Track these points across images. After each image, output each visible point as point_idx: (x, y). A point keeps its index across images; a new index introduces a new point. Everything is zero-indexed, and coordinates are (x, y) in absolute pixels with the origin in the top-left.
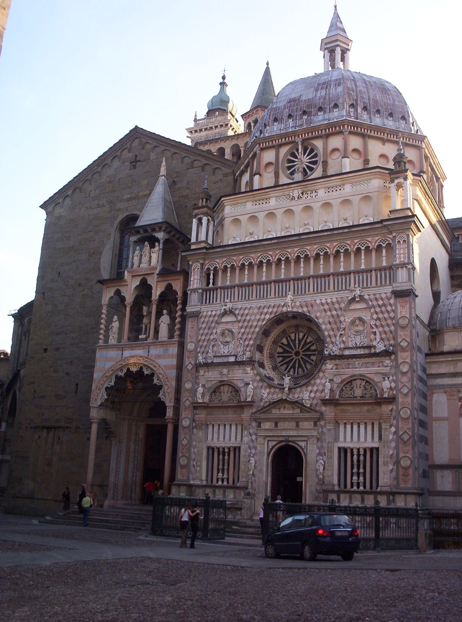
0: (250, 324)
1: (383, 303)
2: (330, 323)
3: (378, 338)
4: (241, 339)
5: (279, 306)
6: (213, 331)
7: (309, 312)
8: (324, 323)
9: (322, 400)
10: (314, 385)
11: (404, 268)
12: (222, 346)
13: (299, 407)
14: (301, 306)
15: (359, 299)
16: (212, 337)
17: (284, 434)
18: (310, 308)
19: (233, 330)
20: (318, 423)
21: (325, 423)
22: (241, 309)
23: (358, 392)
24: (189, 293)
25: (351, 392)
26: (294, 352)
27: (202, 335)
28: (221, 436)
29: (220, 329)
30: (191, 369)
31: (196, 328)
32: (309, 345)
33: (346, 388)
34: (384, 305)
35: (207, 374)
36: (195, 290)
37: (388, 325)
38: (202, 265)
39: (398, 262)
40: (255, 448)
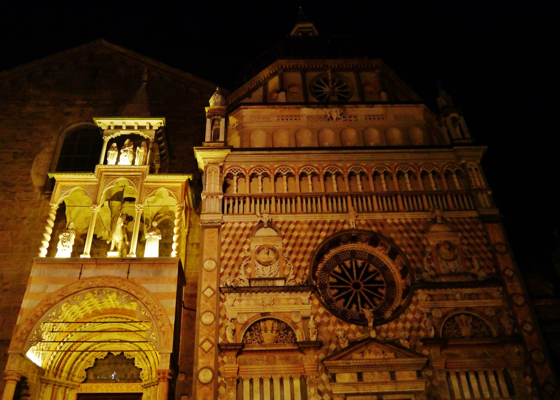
0: (300, 241)
2: (410, 246)
3: (477, 267)
4: (288, 259)
7: (379, 230)
8: (403, 246)
9: (423, 340)
11: (485, 195)
12: (260, 266)
13: (391, 350)
16: (242, 255)
18: (380, 228)
19: (276, 247)
20: (423, 373)
22: (283, 223)
23: (465, 331)
24: (203, 197)
25: (456, 331)
26: (351, 284)
27: (226, 251)
30: (212, 296)
31: (216, 243)
32: (372, 276)
33: (448, 325)
35: (237, 303)
36: (212, 196)
38: (222, 168)
39: (475, 187)
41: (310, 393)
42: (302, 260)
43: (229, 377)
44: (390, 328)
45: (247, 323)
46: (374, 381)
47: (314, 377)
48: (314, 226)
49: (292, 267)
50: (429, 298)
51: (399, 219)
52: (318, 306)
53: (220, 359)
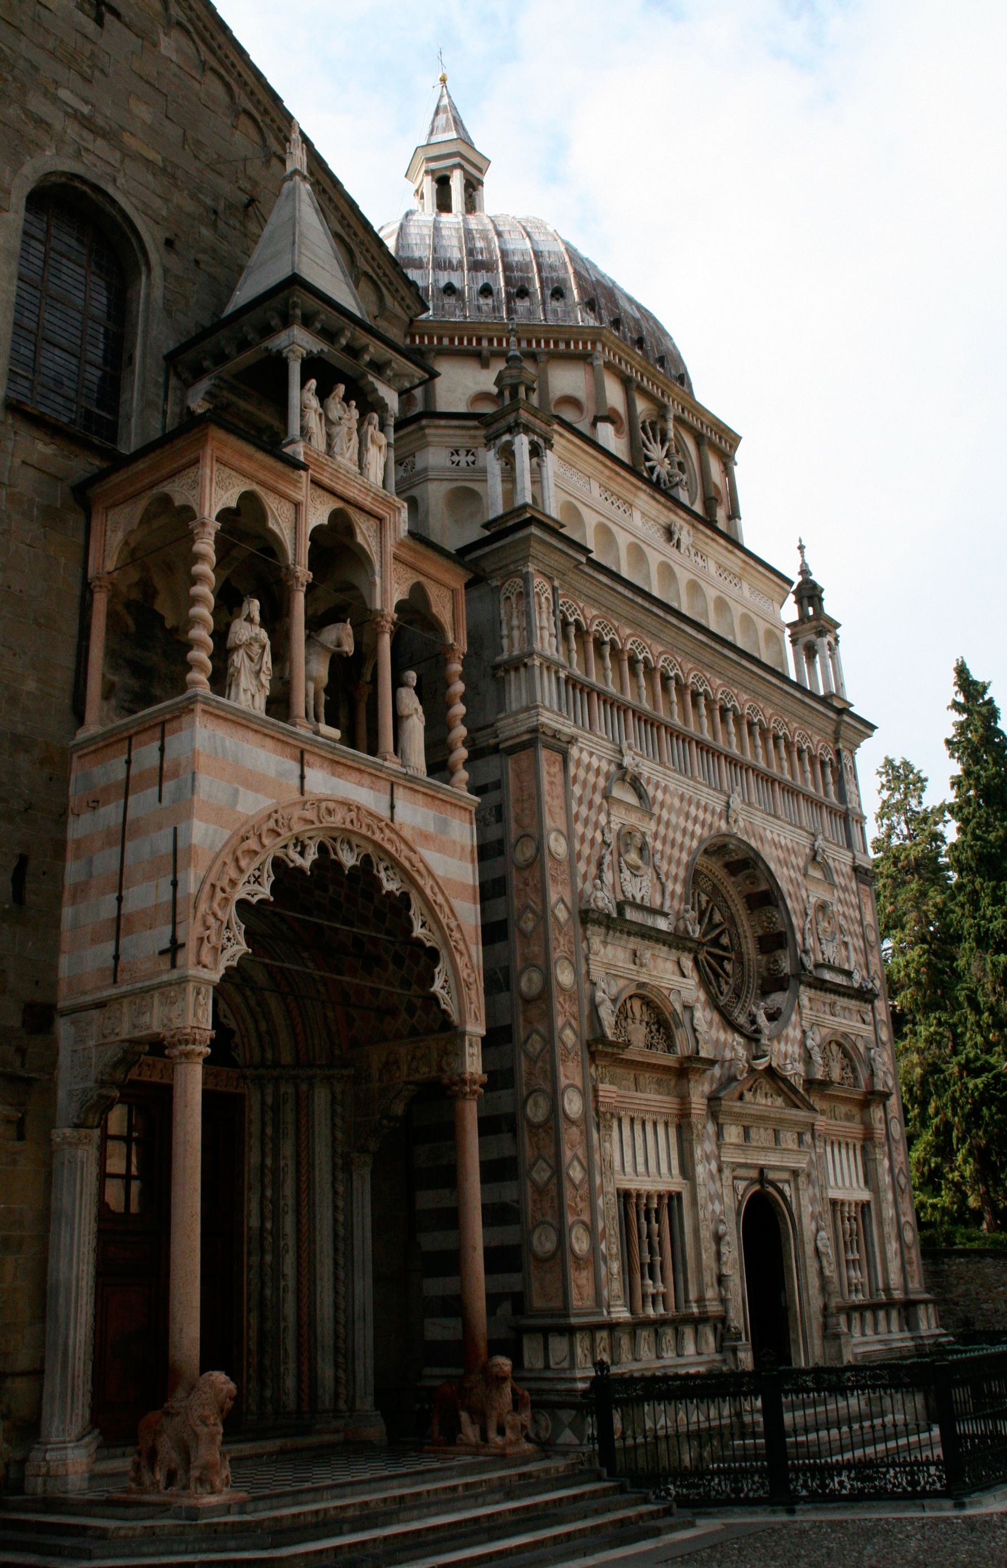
12: (627, 874)
13: (780, 1092)
14: (747, 833)
18: (759, 843)
28: (640, 1160)
35: (602, 950)
40: (720, 1198)
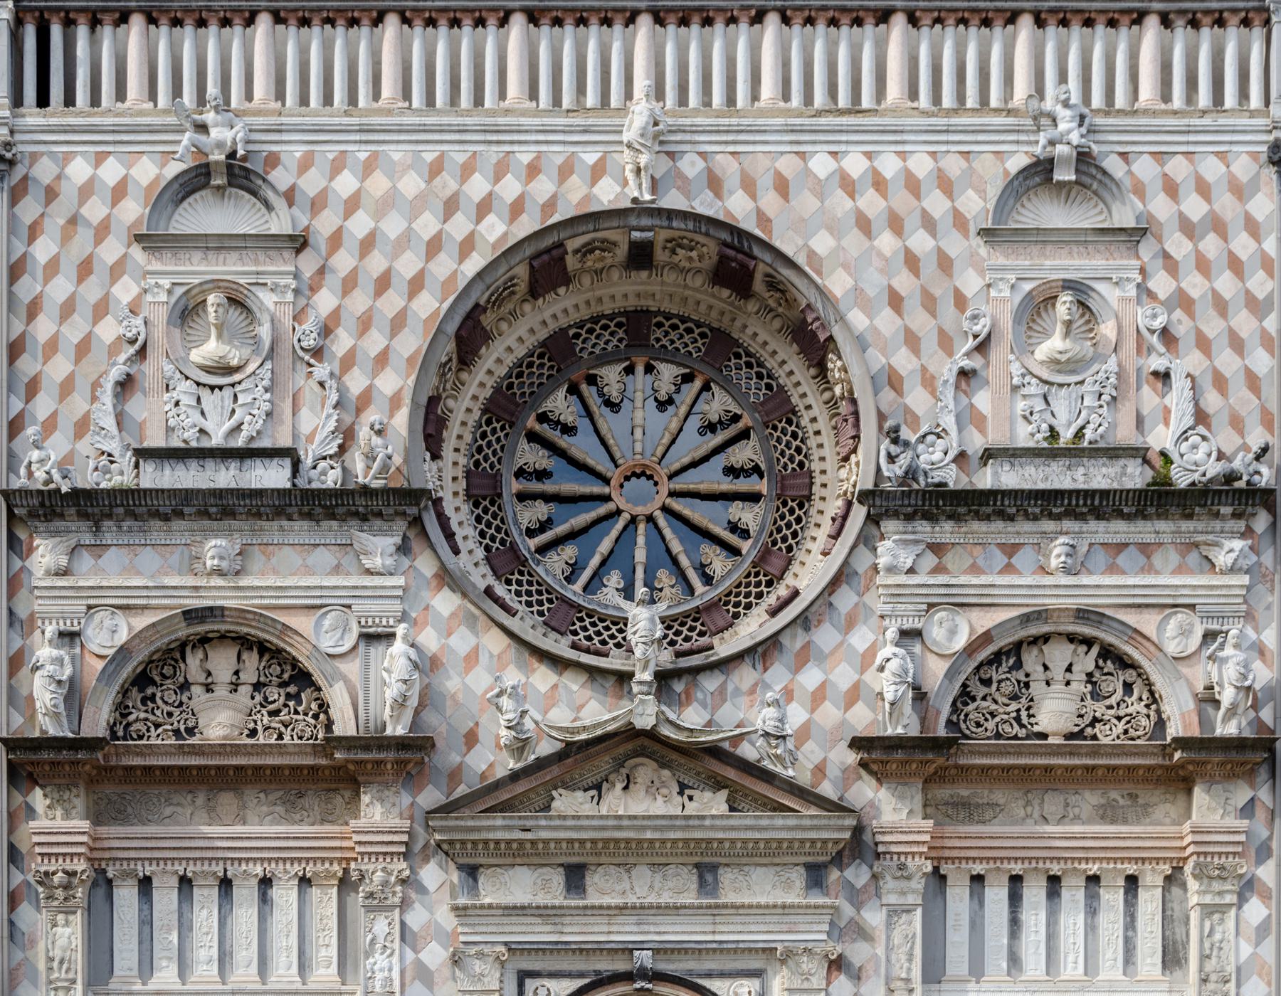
0: (376, 263)
1: (1212, 213)
2: (896, 301)
4: (318, 353)
5: (565, 171)
6: (117, 290)
7: (763, 219)
10: (802, 659)
15: (1073, 178)
17: (625, 932)
18: (770, 201)
20: (834, 874)
21: (875, 877)
29: (166, 282)
34: (1218, 226)
35: (86, 561)
37: (1237, 344)
41: (370, 937)
42: (382, 360)
43: (52, 869)
44: (730, 687)
45: (124, 652)
46: (632, 899)
47: (393, 879)
48: (448, 183)
49: (334, 397)
50: (930, 560)
51: (869, 155)
52: (434, 583)
53: (18, 798)
